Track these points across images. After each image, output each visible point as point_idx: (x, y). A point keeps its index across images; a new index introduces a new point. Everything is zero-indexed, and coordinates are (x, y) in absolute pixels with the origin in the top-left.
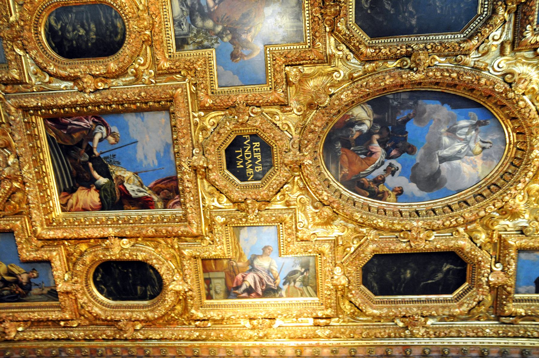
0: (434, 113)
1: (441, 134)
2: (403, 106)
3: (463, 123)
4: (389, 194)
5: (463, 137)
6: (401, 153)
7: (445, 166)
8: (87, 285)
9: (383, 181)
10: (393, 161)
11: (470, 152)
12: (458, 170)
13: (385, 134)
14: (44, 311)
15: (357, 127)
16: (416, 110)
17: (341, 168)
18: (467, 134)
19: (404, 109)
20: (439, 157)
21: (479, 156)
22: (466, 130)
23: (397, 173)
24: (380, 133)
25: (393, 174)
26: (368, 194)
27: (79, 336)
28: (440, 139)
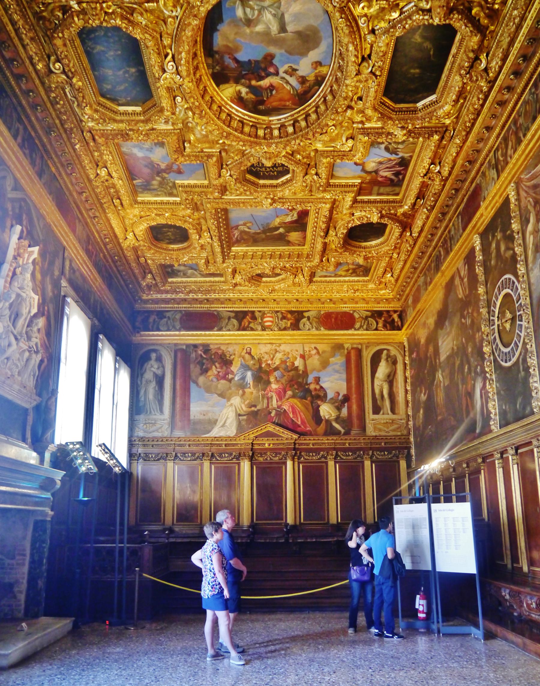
0: (227, 38)
1: (252, 32)
2: (220, 62)
3: (239, 12)
4: (319, 72)
5: (256, 13)
6: (272, 64)
8: (365, 248)
9: (303, 77)
10: (281, 71)
11: (275, 5)
12: (297, 17)
13: (251, 76)
15: (243, 94)
16: (226, 53)
17: (285, 106)
18: (252, 9)
19: (224, 62)
20: (279, 33)
22: (248, 10)
23: (295, 67)
24: (250, 80)
25: (296, 70)
26: (317, 87)
28: (258, 33)
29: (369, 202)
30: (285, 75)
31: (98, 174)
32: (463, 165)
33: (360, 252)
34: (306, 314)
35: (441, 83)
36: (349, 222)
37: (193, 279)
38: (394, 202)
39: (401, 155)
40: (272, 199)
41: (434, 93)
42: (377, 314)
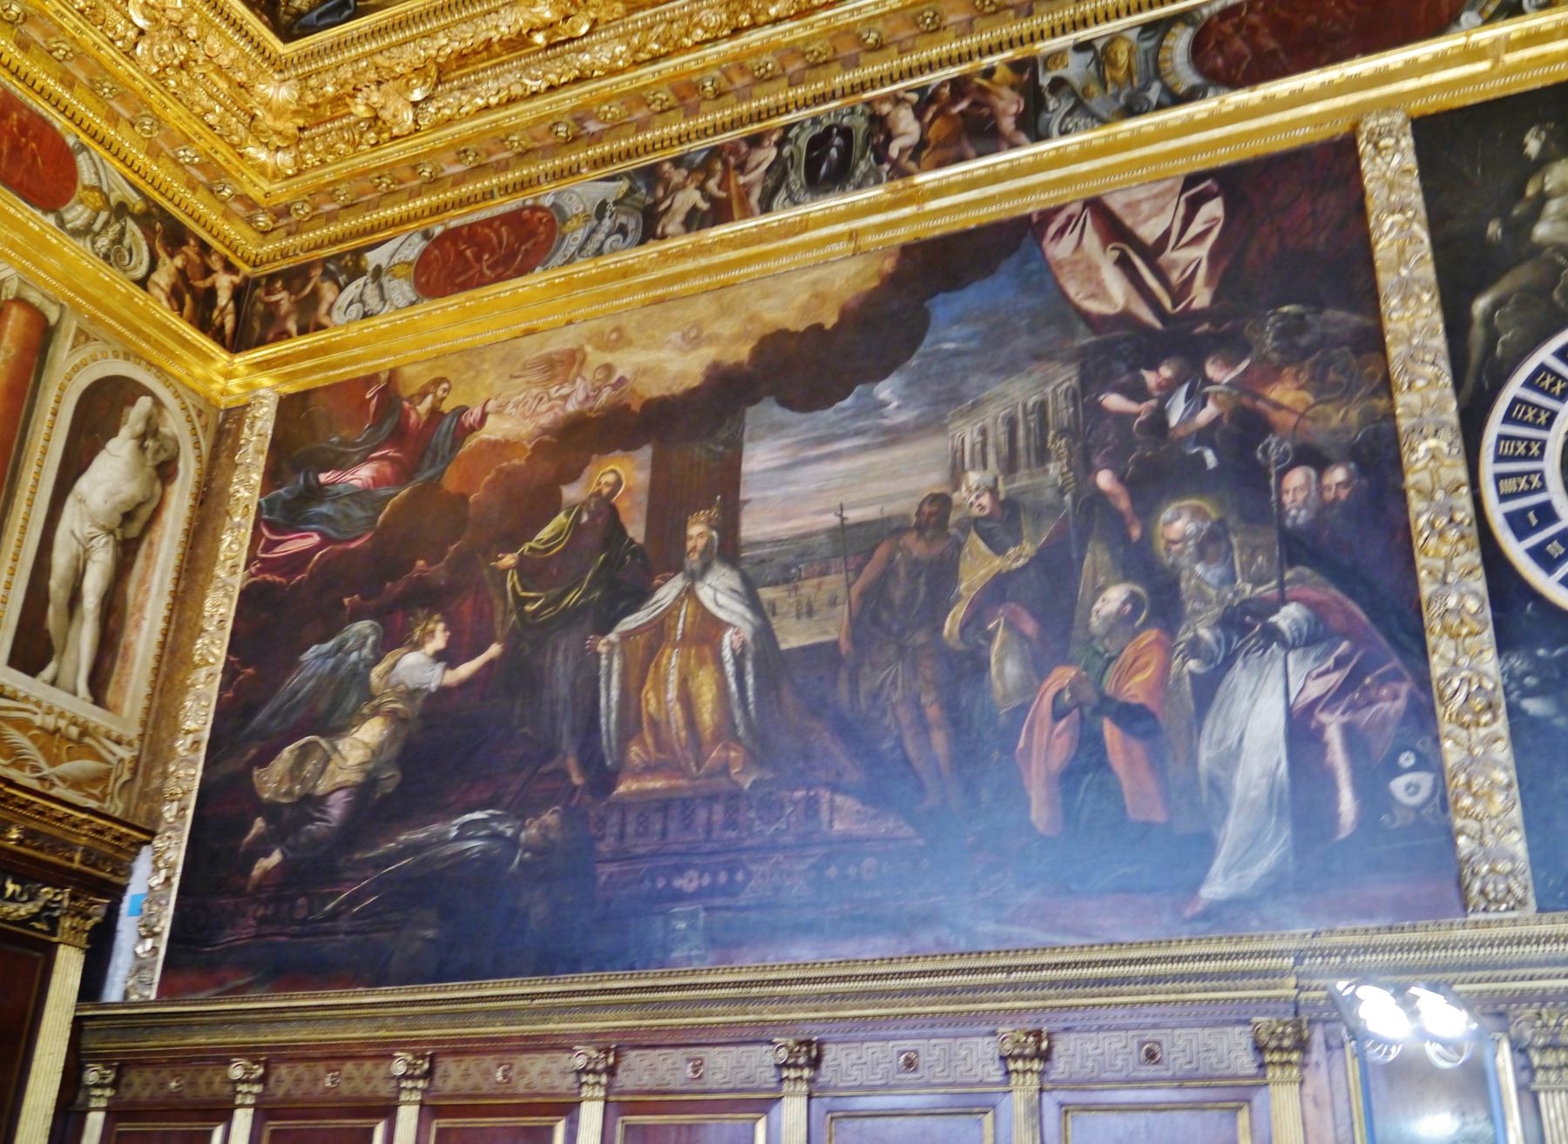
14: (464, 21)
27: (614, 59)
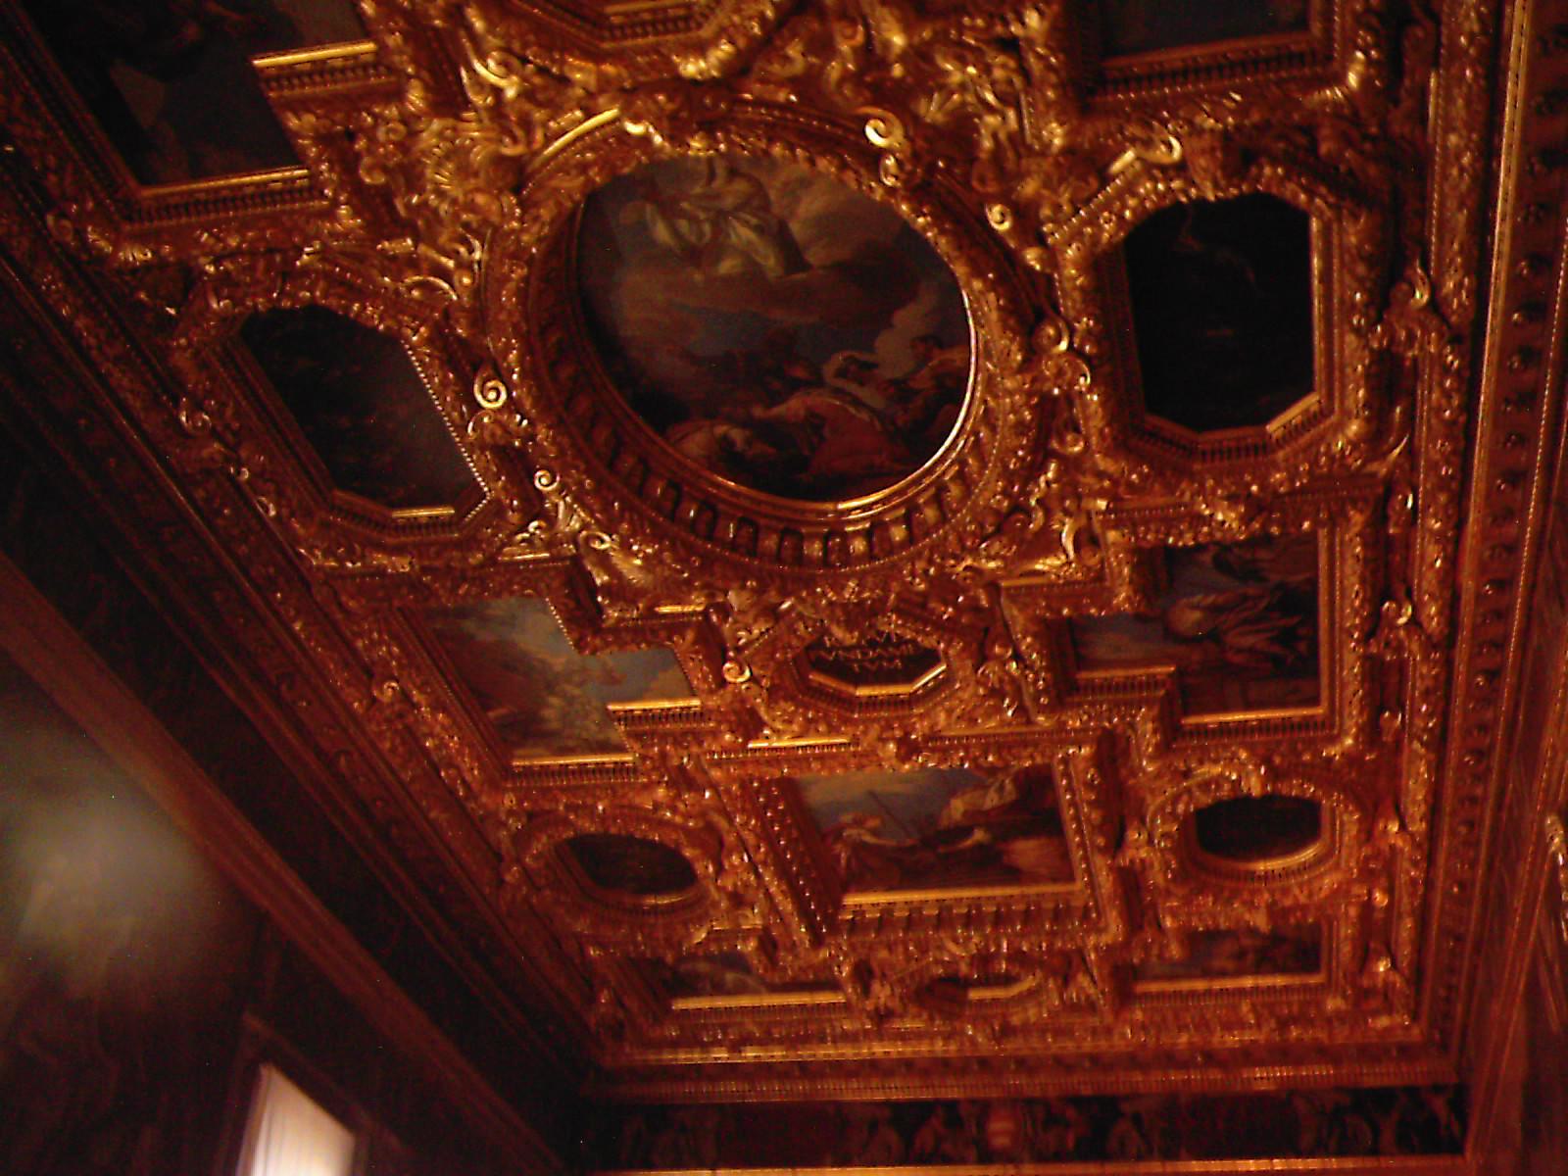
3: (661, 232)
5: (707, 228)
7: (815, 256)
10: (829, 370)
15: (740, 445)
18: (693, 219)
21: (764, 179)
22: (684, 225)
23: (865, 357)
28: (728, 280)
29: (1224, 729)
30: (840, 383)
31: (374, 700)
32: (1480, 597)
33: (1254, 892)
34: (1127, 1108)
35: (1319, 361)
36: (1176, 799)
37: (746, 1001)
38: (1306, 724)
39: (1275, 578)
40: (900, 742)
41: (1309, 389)
42: (1370, 1103)
